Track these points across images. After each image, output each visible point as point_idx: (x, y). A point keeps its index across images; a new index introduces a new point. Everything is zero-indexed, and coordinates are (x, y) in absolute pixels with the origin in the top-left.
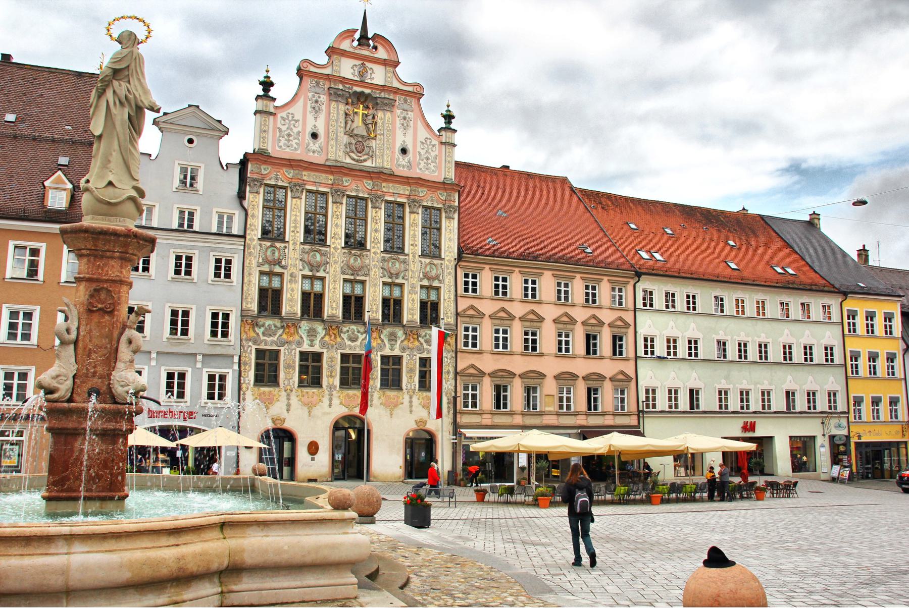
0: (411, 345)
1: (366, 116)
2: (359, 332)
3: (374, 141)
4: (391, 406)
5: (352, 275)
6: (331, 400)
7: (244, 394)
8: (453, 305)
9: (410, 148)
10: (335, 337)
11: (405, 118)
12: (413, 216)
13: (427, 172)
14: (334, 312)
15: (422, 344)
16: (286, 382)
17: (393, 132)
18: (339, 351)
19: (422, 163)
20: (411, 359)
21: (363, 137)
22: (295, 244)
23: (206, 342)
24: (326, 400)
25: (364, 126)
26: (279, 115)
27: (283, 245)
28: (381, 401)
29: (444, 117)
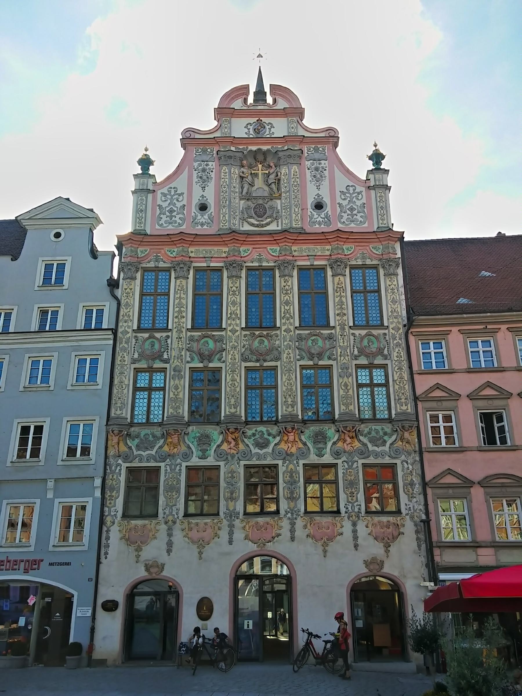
0: (348, 448)
1: (268, 175)
2: (269, 434)
3: (278, 202)
4: (325, 541)
5: (257, 361)
6: (231, 533)
7: (108, 531)
8: (408, 387)
9: (327, 200)
10: (237, 444)
11: (317, 169)
12: (337, 279)
13: (352, 225)
14: (233, 410)
15: (365, 445)
16: (167, 512)
17: (303, 187)
18: (242, 463)
19: (345, 216)
20: (350, 467)
21: (264, 198)
22: (180, 331)
23: (60, 463)
24: (224, 534)
25: (266, 188)
26: (159, 192)
27: (164, 334)
28: (307, 531)
29: (370, 158)
